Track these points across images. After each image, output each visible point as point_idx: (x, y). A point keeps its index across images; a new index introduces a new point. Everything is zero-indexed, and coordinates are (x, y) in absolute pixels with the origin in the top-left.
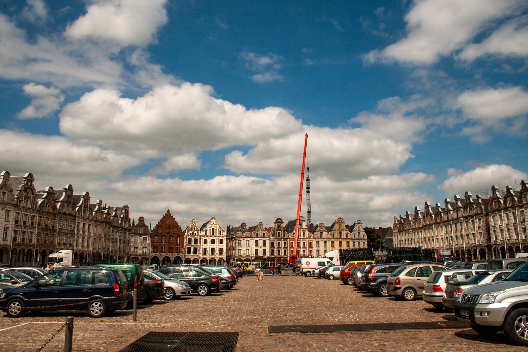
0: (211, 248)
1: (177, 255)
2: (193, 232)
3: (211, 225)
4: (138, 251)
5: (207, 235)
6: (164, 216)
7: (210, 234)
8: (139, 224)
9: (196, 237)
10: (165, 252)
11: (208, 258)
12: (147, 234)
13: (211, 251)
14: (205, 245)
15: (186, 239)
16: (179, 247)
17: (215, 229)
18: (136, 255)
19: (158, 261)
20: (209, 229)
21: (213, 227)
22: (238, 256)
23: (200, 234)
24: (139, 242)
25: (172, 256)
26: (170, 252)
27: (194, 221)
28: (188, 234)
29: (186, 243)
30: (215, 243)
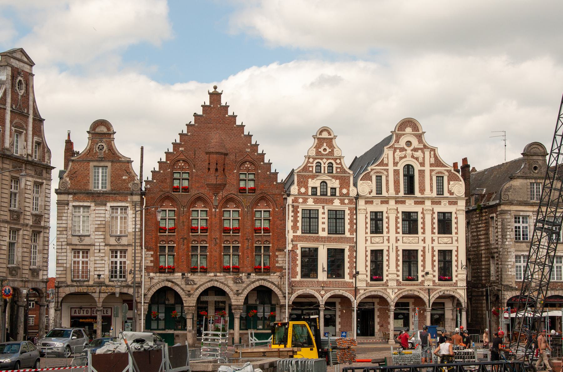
0: (404, 251)
1: (257, 284)
2: (324, 183)
3: (398, 153)
4: (91, 266)
5: (384, 193)
6: (195, 115)
7: (397, 191)
8: (90, 151)
9: (337, 202)
10: (204, 271)
11: (390, 291)
12: (127, 195)
13: (400, 263)
14: (377, 238)
15: (295, 211)
16: (267, 248)
17: (417, 167)
18: (80, 283)
19: (178, 309)
20: (391, 168)
21: (409, 161)
22: (514, 285)
23: (353, 192)
24: (92, 228)
25: (235, 288)
26: (226, 270)
27: (325, 135)
28: (303, 190)
29: (295, 228)
30: (420, 230)
